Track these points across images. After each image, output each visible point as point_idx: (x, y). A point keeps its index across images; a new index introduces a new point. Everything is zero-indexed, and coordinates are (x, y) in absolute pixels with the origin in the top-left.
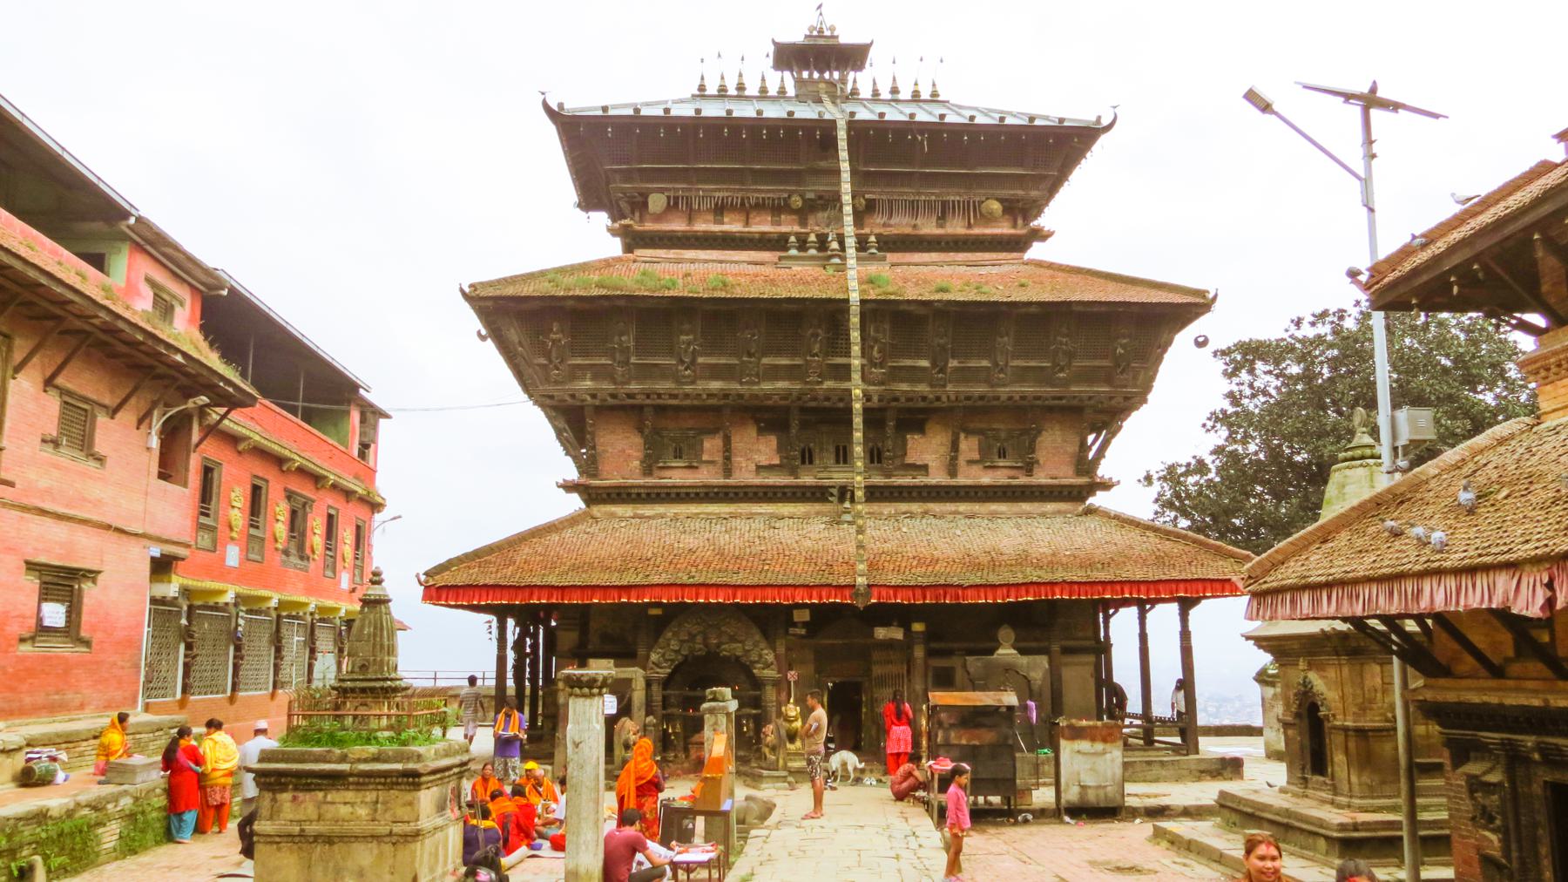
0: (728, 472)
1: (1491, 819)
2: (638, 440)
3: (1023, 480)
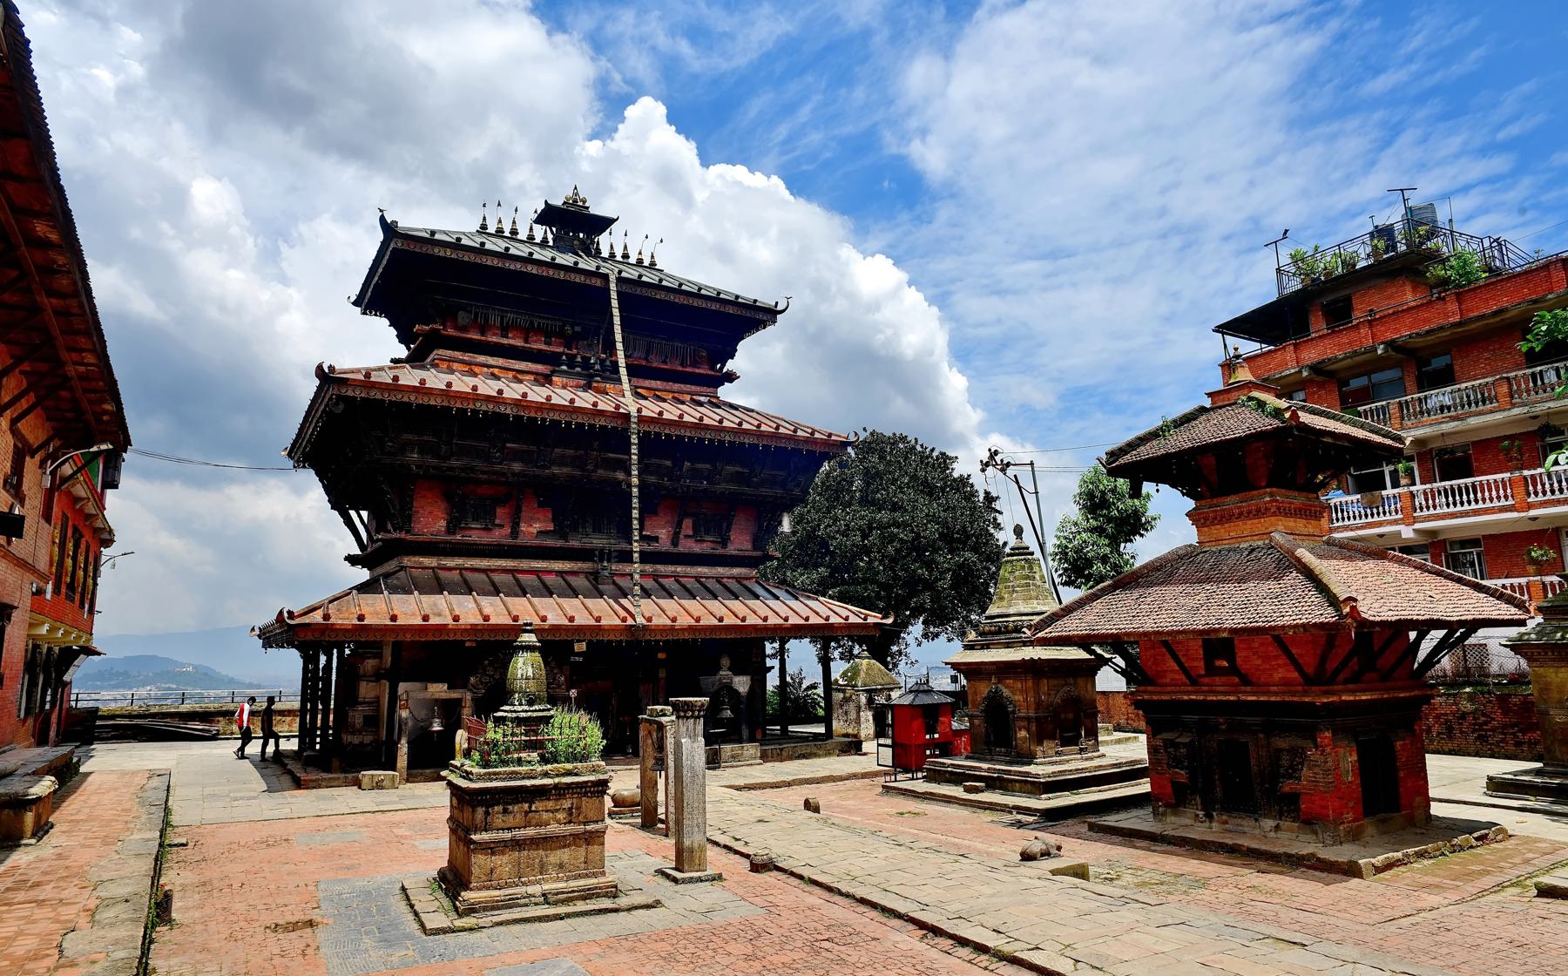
0: (515, 533)
2: (443, 506)
3: (720, 551)
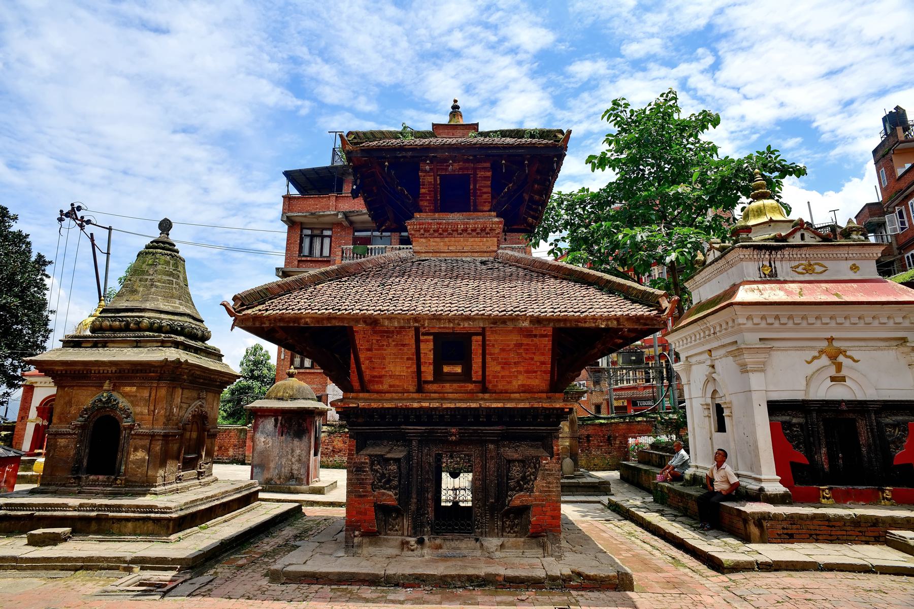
1: (389, 481)
